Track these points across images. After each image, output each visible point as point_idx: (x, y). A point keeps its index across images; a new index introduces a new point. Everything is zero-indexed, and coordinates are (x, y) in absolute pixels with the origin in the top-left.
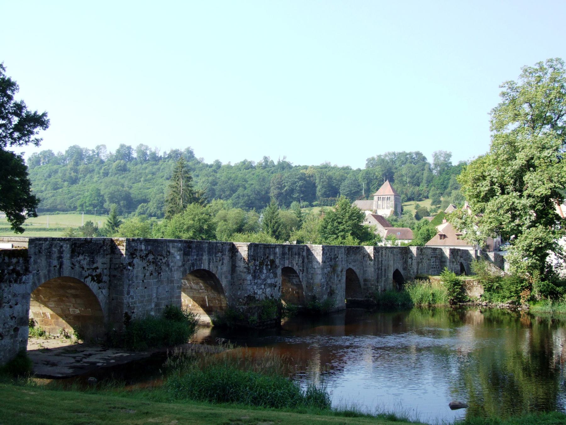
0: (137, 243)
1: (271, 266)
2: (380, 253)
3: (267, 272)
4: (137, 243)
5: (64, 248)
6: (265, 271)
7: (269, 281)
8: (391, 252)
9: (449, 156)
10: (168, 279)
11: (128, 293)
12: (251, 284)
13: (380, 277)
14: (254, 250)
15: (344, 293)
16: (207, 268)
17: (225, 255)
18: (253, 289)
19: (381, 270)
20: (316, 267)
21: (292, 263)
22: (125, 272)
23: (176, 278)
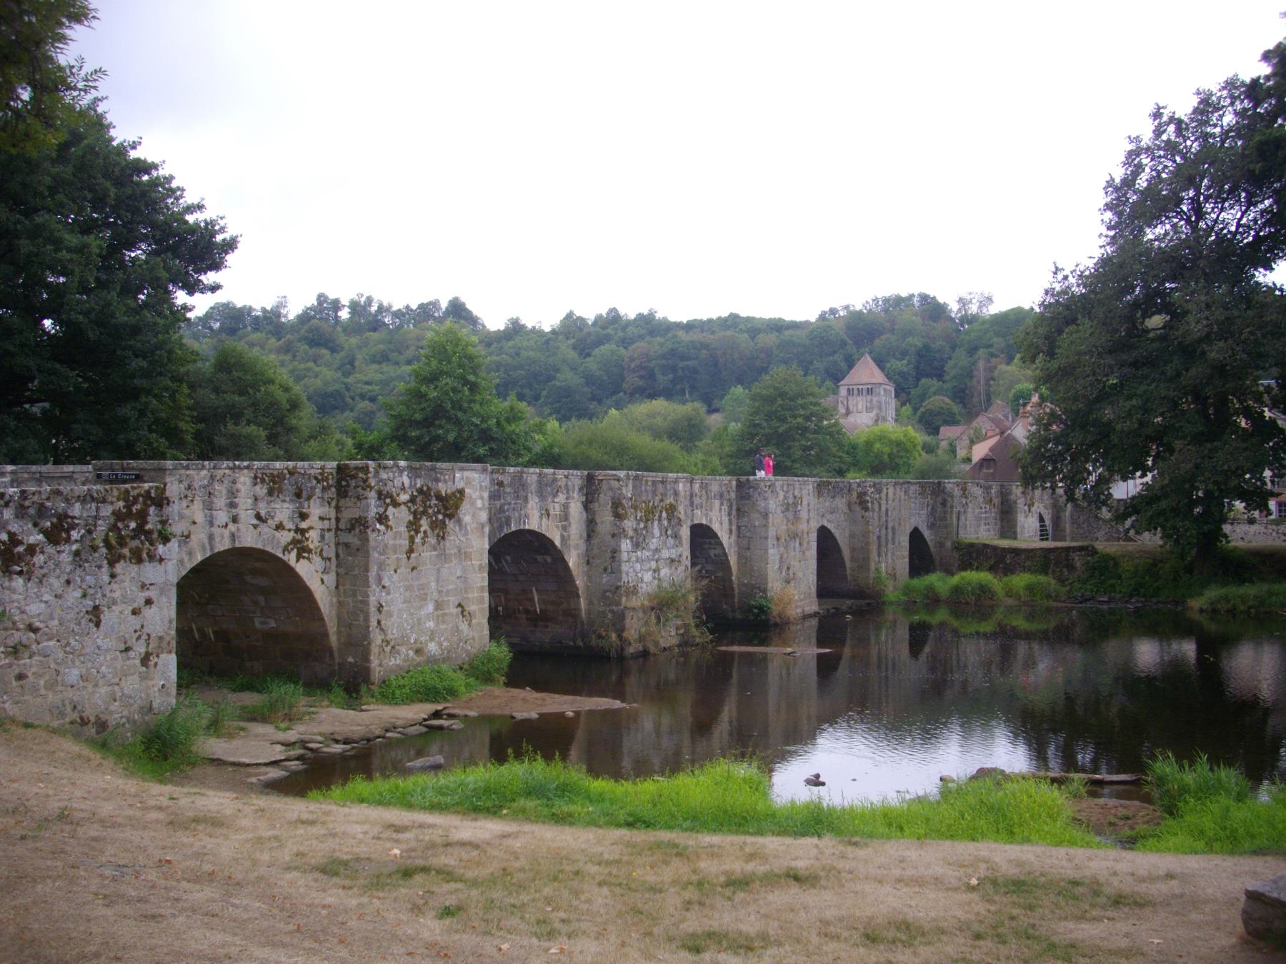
0: (394, 473)
1: (669, 520)
2: (883, 496)
3: (661, 535)
4: (394, 473)
5: (239, 486)
6: (656, 532)
7: (665, 554)
8: (905, 492)
9: (990, 299)
11: (379, 579)
12: (628, 561)
13: (884, 543)
14: (634, 487)
15: (815, 578)
16: (536, 529)
17: (573, 498)
18: (634, 571)
19: (887, 528)
20: (757, 524)
21: (707, 515)
22: (372, 536)
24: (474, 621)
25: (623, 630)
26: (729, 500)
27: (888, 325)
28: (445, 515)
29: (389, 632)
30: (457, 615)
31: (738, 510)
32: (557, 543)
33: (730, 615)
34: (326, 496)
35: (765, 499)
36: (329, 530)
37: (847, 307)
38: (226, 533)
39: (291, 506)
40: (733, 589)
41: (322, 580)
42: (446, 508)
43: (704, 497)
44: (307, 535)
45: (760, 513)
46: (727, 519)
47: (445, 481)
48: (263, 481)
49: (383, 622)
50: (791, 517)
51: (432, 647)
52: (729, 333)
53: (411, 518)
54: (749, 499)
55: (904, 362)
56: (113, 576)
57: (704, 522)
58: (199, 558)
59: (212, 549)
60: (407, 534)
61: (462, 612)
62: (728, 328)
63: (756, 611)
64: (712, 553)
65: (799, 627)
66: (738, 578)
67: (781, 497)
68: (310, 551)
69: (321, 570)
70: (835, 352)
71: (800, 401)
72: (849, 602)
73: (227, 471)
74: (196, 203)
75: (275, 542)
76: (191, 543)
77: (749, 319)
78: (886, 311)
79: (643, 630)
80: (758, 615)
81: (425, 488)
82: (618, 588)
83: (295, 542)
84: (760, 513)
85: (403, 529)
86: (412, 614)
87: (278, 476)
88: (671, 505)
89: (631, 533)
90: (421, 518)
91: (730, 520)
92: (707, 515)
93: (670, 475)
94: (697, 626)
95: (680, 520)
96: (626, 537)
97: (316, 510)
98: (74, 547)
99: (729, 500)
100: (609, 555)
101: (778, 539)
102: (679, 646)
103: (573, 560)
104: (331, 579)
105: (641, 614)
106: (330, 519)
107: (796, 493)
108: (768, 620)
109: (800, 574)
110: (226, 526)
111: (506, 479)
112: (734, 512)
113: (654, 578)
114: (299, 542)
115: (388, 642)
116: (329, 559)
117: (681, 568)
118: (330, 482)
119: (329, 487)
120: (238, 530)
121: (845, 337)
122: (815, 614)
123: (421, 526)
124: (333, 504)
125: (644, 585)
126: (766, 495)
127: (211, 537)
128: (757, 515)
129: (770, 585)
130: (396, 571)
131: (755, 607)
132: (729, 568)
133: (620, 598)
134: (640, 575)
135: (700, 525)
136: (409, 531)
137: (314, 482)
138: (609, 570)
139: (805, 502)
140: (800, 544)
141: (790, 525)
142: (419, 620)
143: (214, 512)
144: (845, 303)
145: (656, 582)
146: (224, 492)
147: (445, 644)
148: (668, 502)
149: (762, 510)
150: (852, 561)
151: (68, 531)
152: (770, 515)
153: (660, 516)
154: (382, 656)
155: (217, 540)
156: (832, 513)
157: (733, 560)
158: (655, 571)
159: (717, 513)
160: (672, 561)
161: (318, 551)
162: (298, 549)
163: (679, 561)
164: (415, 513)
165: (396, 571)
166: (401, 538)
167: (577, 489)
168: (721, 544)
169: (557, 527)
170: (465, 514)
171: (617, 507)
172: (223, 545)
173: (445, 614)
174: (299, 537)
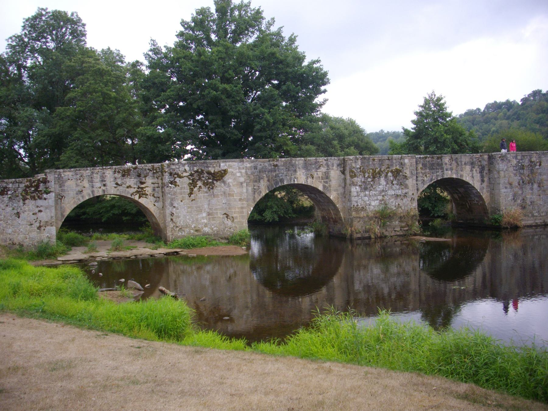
0: (179, 166)
3: (387, 183)
4: (179, 166)
5: (106, 174)
10: (224, 193)
11: (172, 205)
14: (362, 163)
18: (363, 200)
20: (496, 176)
23: (236, 192)
24: (235, 220)
28: (213, 180)
29: (178, 223)
30: (223, 218)
31: (489, 170)
32: (321, 188)
34: (155, 175)
35: (498, 164)
36: (158, 187)
38: (100, 190)
39: (135, 180)
41: (155, 205)
42: (214, 177)
44: (144, 189)
46: (479, 175)
47: (214, 167)
48: (119, 172)
49: (174, 220)
51: (206, 230)
53: (191, 182)
56: (24, 204)
58: (87, 198)
59: (93, 194)
60: (189, 188)
61: (227, 217)
68: (147, 195)
69: (153, 201)
73: (100, 170)
74: (316, 59)
75: (128, 193)
76: (83, 194)
81: (200, 170)
83: (137, 192)
85: (186, 186)
86: (193, 217)
87: (127, 170)
90: (197, 181)
93: (395, 156)
95: (406, 176)
97: (149, 181)
98: (9, 196)
101: (511, 184)
103: (333, 196)
104: (159, 204)
106: (158, 183)
110: (100, 188)
111: (279, 163)
114: (140, 191)
115: (177, 227)
116: (159, 197)
118: (158, 170)
119: (157, 172)
120: (106, 189)
123: (197, 184)
124: (160, 178)
127: (93, 192)
130: (182, 201)
136: (190, 187)
137: (148, 171)
142: (197, 220)
143: (94, 184)
146: (99, 177)
147: (215, 228)
148: (394, 168)
149: (498, 170)
151: (7, 192)
154: (173, 231)
155: (96, 192)
157: (485, 195)
161: (152, 195)
162: (140, 194)
164: (193, 180)
165: (182, 201)
166: (185, 189)
167: (335, 165)
169: (321, 182)
170: (228, 179)
172: (99, 193)
173: (215, 217)
174: (140, 190)
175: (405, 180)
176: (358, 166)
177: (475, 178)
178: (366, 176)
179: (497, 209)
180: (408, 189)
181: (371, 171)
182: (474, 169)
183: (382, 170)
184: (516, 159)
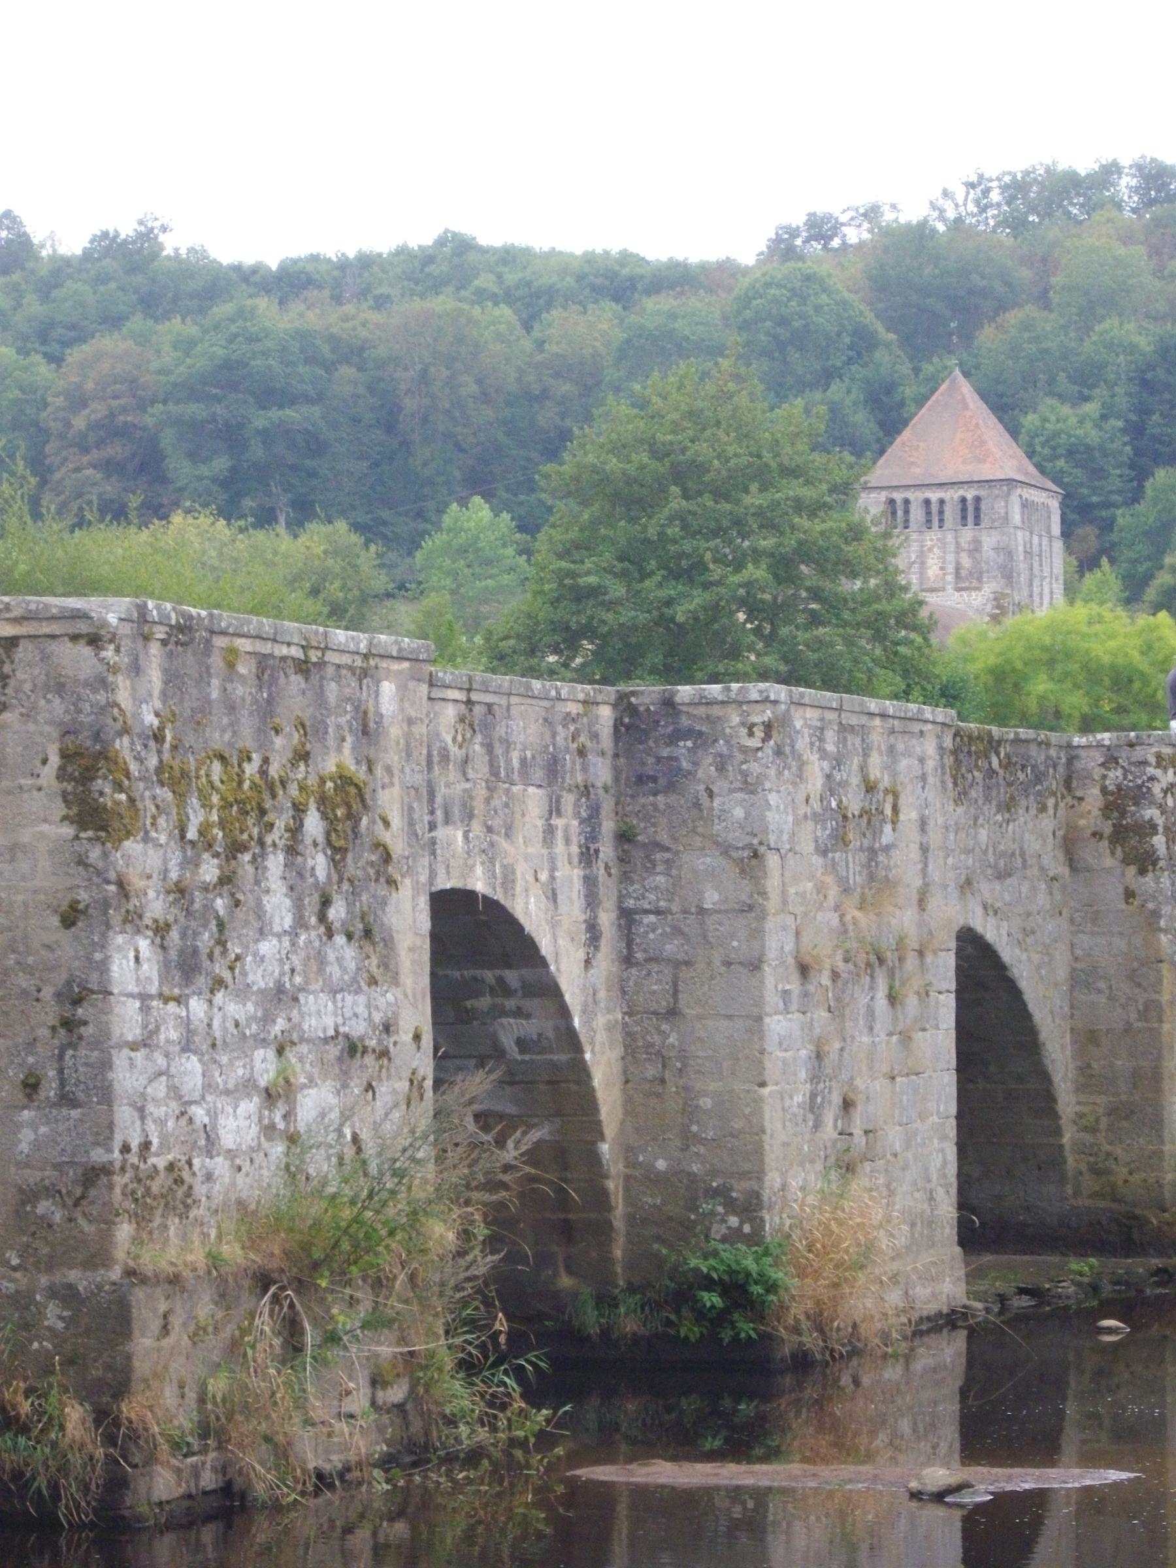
1: (337, 854)
3: (300, 922)
12: (146, 1043)
14: (171, 678)
18: (174, 1091)
20: (711, 898)
21: (490, 853)
25: (121, 1386)
26: (586, 790)
27: (1025, 274)
31: (624, 837)
33: (591, 1320)
35: (750, 786)
37: (871, 214)
40: (601, 1199)
43: (479, 769)
45: (726, 850)
46: (577, 874)
50: (857, 878)
52: (442, 303)
54: (671, 788)
55: (1091, 408)
57: (480, 886)
62: (436, 286)
63: (712, 1299)
64: (509, 1031)
65: (893, 1373)
66: (628, 1152)
67: (815, 783)
70: (827, 377)
71: (754, 499)
72: (1083, 1266)
77: (509, 256)
78: (1017, 224)
79: (218, 1386)
80: (721, 1318)
82: (95, 1175)
84: (726, 850)
88: (344, 781)
89: (156, 906)
91: (590, 882)
92: (490, 853)
94: (468, 1367)
95: (387, 857)
96: (133, 920)
99: (586, 790)
100: (48, 1013)
101: (804, 970)
102: (387, 1463)
105: (205, 1308)
107: (875, 771)
108: (767, 1338)
109: (893, 1137)
112: (607, 850)
113: (269, 1130)
117: (392, 1088)
121: (869, 318)
122: (951, 1320)
125: (220, 1165)
126: (754, 768)
128: (708, 861)
129: (773, 1179)
131: (708, 1283)
132: (588, 1103)
133: (107, 1222)
134: (199, 1113)
135: (465, 897)
138: (50, 1090)
139: (909, 815)
140: (892, 999)
141: (852, 913)
144: (863, 201)
145: (278, 1149)
148: (330, 766)
149: (737, 837)
150: (1079, 1089)
152: (772, 860)
153: (295, 831)
156: (1001, 875)
158: (270, 1096)
159: (536, 848)
160: (353, 1048)
163: (384, 1054)
168: (552, 991)
171: (87, 776)
175: (382, 890)
176: (150, 719)
177: (563, 909)
178: (192, 834)
179: (721, 1193)
180: (395, 981)
181: (217, 766)
182: (559, 822)
183: (274, 771)
184: (823, 754)
